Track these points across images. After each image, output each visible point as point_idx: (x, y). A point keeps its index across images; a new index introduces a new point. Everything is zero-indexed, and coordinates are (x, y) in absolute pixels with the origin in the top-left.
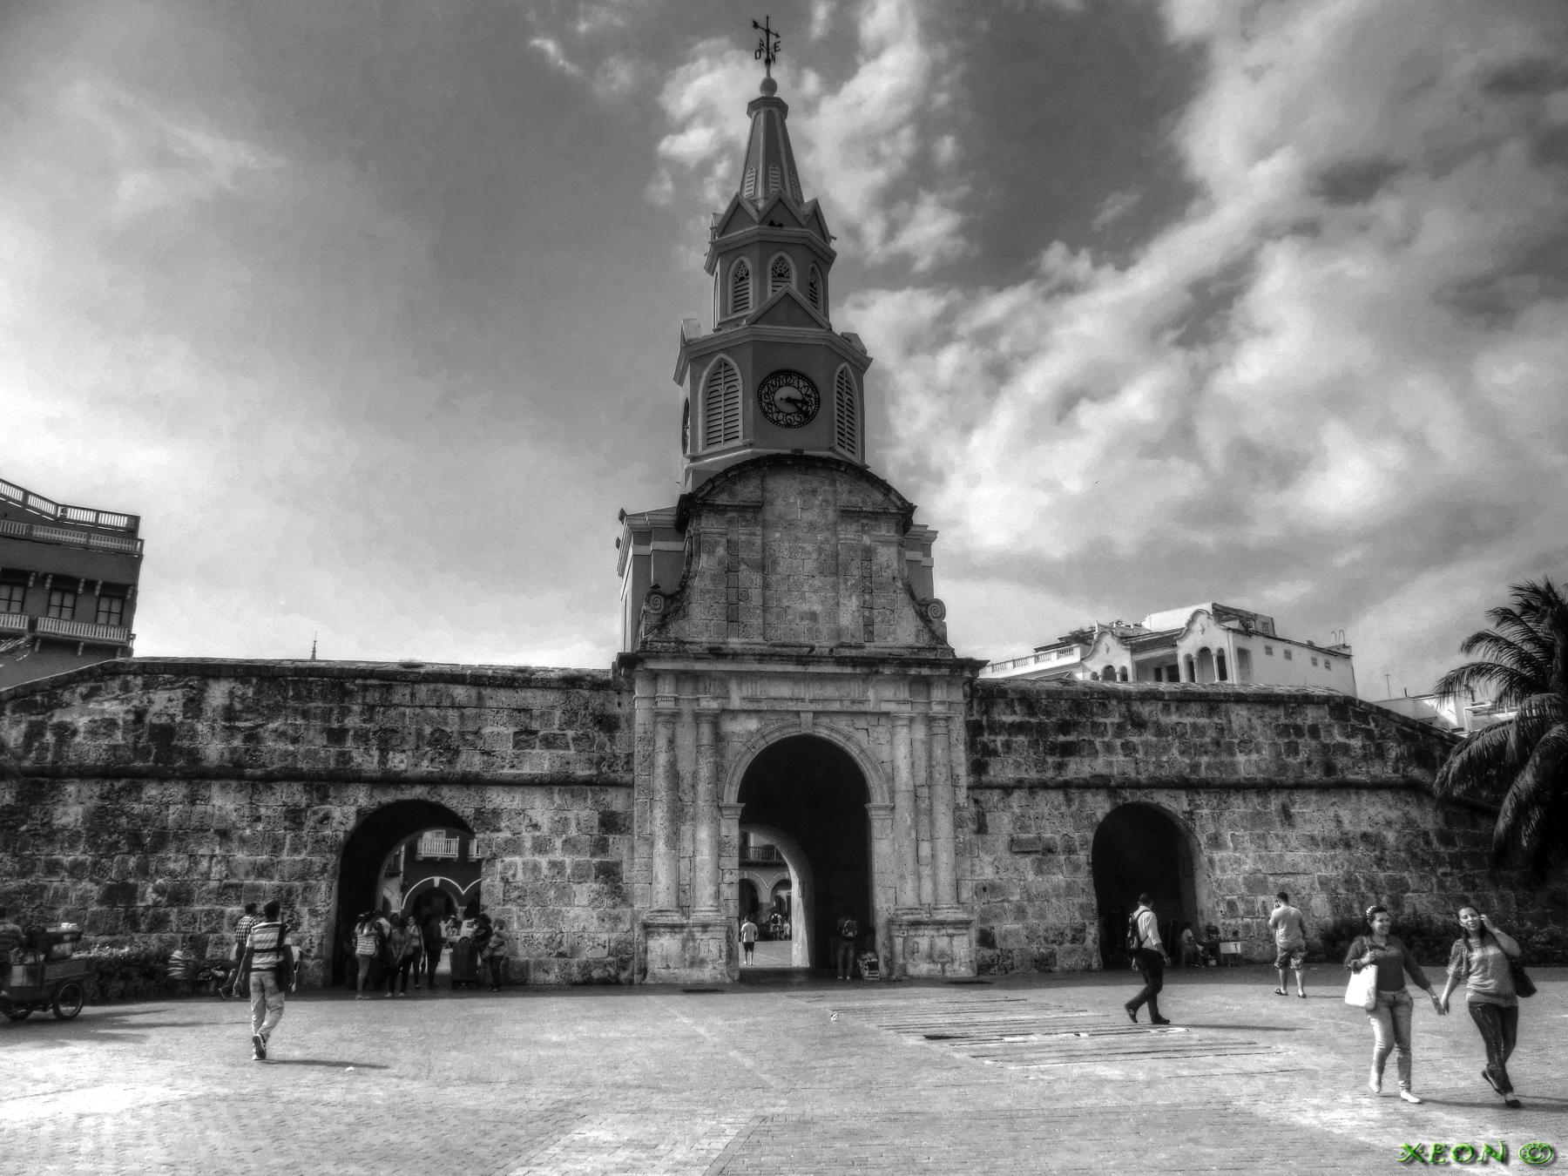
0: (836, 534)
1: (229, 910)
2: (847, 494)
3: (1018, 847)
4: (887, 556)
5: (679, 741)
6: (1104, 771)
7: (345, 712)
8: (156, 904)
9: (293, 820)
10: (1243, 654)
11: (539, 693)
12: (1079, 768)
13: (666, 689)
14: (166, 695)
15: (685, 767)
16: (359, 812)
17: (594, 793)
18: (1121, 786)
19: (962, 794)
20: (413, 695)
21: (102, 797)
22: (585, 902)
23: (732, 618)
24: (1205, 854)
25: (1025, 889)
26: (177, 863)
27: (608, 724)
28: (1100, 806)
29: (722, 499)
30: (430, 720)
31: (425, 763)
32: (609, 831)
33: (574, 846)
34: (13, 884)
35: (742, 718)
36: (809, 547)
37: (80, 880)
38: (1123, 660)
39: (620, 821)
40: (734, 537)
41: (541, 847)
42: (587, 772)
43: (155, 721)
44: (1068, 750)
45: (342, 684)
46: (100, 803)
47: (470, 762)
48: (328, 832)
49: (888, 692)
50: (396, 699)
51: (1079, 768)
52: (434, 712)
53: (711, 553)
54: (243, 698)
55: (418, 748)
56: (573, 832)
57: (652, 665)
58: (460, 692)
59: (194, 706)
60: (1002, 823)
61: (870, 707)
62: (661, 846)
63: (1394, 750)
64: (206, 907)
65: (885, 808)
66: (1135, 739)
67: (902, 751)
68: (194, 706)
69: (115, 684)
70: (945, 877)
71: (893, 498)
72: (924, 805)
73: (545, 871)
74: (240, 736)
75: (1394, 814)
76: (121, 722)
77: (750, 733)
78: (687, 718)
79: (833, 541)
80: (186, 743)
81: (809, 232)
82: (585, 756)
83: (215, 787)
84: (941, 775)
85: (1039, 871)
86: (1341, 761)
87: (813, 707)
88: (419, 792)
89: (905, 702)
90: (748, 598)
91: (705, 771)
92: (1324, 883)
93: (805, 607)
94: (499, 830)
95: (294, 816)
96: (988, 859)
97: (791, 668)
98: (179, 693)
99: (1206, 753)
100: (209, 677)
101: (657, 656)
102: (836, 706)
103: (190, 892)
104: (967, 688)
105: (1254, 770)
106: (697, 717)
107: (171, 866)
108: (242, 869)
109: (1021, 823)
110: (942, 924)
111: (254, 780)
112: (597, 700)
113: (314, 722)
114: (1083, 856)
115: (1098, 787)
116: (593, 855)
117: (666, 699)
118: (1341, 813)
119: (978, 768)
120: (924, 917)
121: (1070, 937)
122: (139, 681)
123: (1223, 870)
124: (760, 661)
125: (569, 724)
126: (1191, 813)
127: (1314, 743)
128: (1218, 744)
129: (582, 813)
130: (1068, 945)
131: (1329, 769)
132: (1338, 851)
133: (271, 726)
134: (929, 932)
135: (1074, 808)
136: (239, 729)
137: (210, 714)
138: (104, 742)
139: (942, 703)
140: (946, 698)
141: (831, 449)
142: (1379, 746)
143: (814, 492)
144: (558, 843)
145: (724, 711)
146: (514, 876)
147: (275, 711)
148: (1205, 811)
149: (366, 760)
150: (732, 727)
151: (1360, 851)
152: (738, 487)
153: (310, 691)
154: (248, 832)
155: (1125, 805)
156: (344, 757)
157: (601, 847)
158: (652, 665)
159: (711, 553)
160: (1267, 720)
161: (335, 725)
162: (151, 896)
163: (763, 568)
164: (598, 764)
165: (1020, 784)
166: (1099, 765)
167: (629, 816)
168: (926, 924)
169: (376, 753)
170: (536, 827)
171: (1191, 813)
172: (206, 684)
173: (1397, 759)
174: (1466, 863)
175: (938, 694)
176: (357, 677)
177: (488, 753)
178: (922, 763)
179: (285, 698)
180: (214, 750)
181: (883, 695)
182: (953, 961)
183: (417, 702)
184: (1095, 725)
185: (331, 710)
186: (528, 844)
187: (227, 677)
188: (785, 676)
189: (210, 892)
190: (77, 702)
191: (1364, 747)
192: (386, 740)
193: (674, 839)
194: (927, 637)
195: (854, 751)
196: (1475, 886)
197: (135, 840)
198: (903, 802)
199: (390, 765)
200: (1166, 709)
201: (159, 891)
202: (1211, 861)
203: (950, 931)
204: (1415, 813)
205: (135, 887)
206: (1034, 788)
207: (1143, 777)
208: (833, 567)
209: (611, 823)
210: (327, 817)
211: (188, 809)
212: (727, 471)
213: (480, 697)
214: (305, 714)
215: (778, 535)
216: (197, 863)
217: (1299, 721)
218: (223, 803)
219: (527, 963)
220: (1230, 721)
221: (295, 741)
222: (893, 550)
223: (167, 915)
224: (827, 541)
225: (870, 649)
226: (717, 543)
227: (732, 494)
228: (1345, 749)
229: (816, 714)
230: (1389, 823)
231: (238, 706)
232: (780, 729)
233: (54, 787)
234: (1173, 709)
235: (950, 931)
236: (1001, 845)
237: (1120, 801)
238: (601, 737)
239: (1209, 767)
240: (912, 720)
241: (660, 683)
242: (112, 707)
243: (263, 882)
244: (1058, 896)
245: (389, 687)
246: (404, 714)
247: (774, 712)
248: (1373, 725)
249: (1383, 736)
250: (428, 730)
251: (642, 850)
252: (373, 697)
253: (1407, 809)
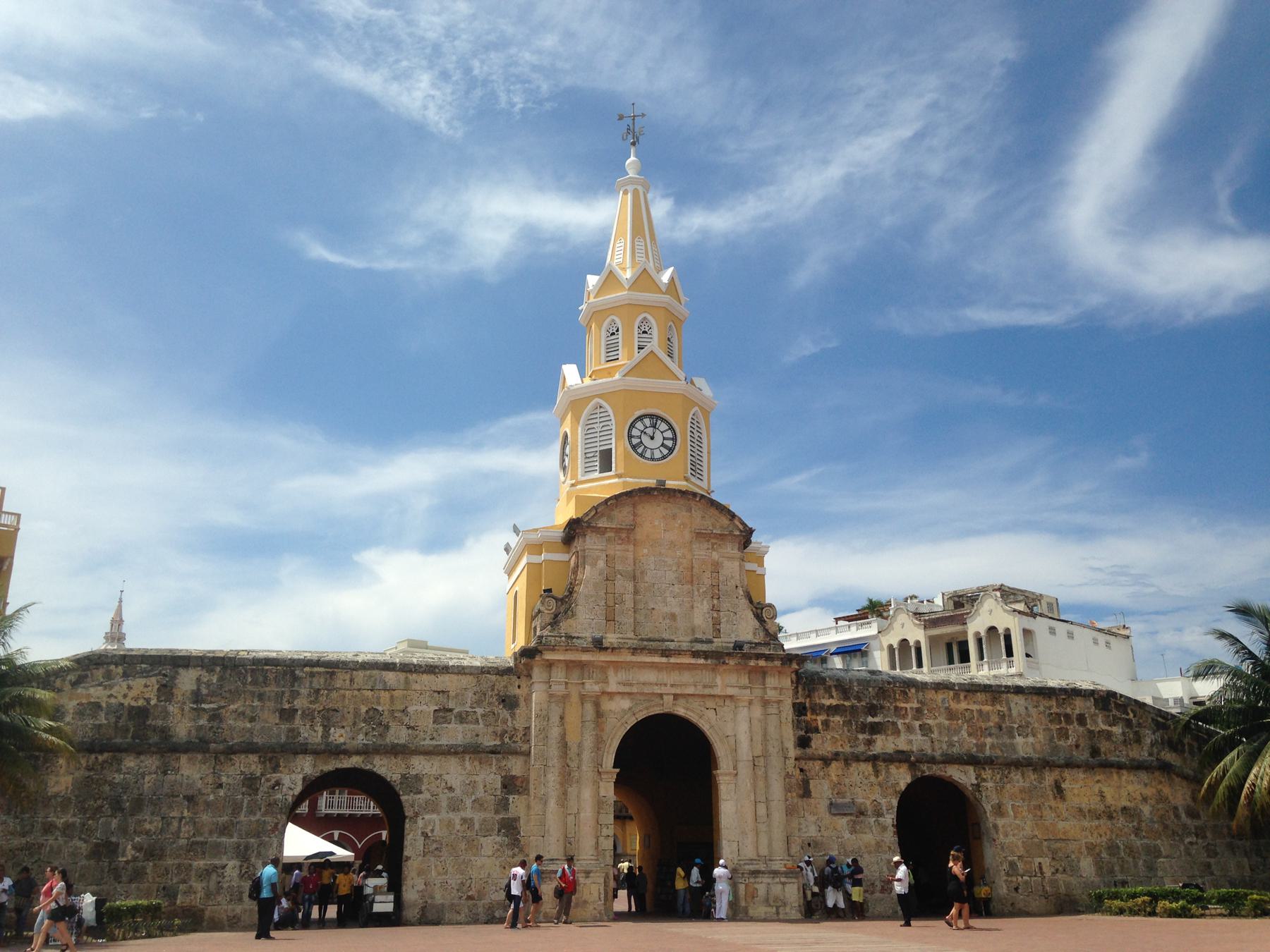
0: (691, 550)
1: (195, 864)
2: (699, 518)
3: (836, 809)
4: (731, 568)
5: (568, 719)
6: (903, 746)
7: (295, 695)
8: (135, 859)
9: (249, 787)
10: (1027, 633)
11: (455, 677)
12: (883, 744)
13: (559, 675)
14: (143, 681)
15: (572, 739)
16: (304, 779)
17: (498, 760)
18: (919, 761)
19: (791, 762)
20: (352, 680)
21: (89, 769)
22: (490, 853)
23: (610, 619)
24: (991, 818)
25: (842, 845)
26: (152, 824)
27: (510, 703)
28: (902, 777)
29: (602, 523)
30: (365, 701)
31: (361, 736)
32: (509, 793)
33: (481, 805)
34: (16, 842)
35: (618, 698)
36: (670, 561)
37: (72, 838)
38: (916, 634)
39: (518, 783)
40: (611, 552)
41: (455, 806)
42: (492, 743)
43: (133, 704)
44: (875, 729)
45: (293, 672)
46: (87, 774)
47: (398, 735)
48: (279, 796)
49: (732, 679)
50: (338, 684)
51: (883, 744)
52: (369, 693)
53: (594, 565)
54: (208, 685)
55: (354, 724)
56: (480, 793)
57: (549, 656)
58: (390, 677)
59: (166, 690)
60: (822, 789)
61: (717, 691)
62: (552, 804)
63: (1149, 737)
64: (176, 862)
65: (730, 774)
66: (929, 722)
67: (743, 728)
68: (166, 690)
69: (99, 673)
70: (778, 835)
71: (737, 523)
72: (760, 772)
73: (458, 827)
74: (206, 717)
75: (1149, 792)
76: (104, 705)
77: (624, 710)
78: (575, 698)
79: (689, 557)
80: (160, 723)
81: (667, 298)
82: (491, 729)
83: (184, 758)
84: (773, 750)
85: (853, 831)
86: (1104, 746)
87: (674, 691)
88: (355, 761)
89: (745, 688)
90: (622, 602)
91: (589, 742)
92: (1091, 848)
93: (666, 610)
94: (421, 792)
95: (251, 783)
96: (813, 819)
97: (657, 659)
98: (153, 680)
99: (990, 735)
100: (179, 666)
101: (553, 649)
102: (691, 690)
103: (162, 849)
104: (794, 676)
105: (1030, 750)
106: (583, 698)
107: (147, 826)
108: (206, 829)
109: (838, 789)
110: (775, 873)
111: (217, 754)
112: (501, 682)
113: (268, 704)
114: (889, 819)
115: (900, 761)
116: (497, 812)
117: (559, 683)
118: (1104, 789)
119: (803, 742)
120: (762, 867)
121: (879, 888)
122: (120, 670)
123: (1006, 835)
124: (633, 654)
125: (479, 703)
126: (978, 785)
127: (1081, 729)
128: (1000, 728)
129: (489, 777)
130: (878, 895)
131: (1095, 752)
132: (1102, 821)
133: (232, 707)
134: (766, 879)
135: (881, 778)
136: (204, 710)
137: (180, 698)
138: (90, 722)
139: (775, 688)
140: (780, 686)
141: (686, 479)
142: (1136, 733)
143: (674, 517)
144: (468, 803)
145: (603, 693)
146: (432, 831)
147: (235, 694)
148: (990, 784)
149: (312, 734)
150: (607, 705)
151: (1121, 821)
152: (615, 513)
153: (266, 678)
154: (212, 797)
155: (923, 777)
156: (293, 733)
157: (503, 805)
158: (549, 656)
159: (594, 565)
160: (1041, 709)
161: (287, 706)
162: (130, 852)
163: (634, 578)
164: (502, 736)
165: (836, 756)
166: (902, 743)
167: (526, 780)
168: (763, 873)
169: (320, 729)
170: (451, 789)
171: (978, 785)
172: (177, 673)
173: (1152, 745)
174: (1209, 834)
175: (771, 681)
176: (305, 665)
177: (413, 728)
178: (758, 738)
179: (244, 684)
180: (182, 728)
181: (727, 681)
182: (785, 905)
183: (355, 686)
184: (896, 708)
185: (283, 693)
186: (444, 804)
187: (195, 667)
188: (653, 666)
189: (181, 848)
190: (67, 687)
191: (1124, 733)
192: (329, 718)
193: (564, 797)
194: (762, 634)
195: (704, 726)
196: (1216, 854)
197: (117, 806)
198: (745, 770)
199: (331, 739)
200: (956, 697)
201: (138, 848)
202: (995, 826)
203: (783, 880)
204: (1166, 791)
205: (117, 845)
206: (850, 759)
207: (938, 754)
208: (689, 578)
209: (511, 785)
210: (278, 783)
211: (160, 777)
212: (607, 500)
213: (407, 682)
214: (261, 697)
215: (645, 551)
216: (168, 825)
217: (1069, 710)
218: (191, 771)
219: (443, 905)
220: (1010, 709)
221: (252, 720)
222: (737, 564)
223: (144, 868)
224: (684, 557)
225: (718, 644)
226: (598, 558)
227: (610, 518)
228: (1109, 735)
229: (676, 696)
230: (1145, 799)
231: (204, 691)
232: (647, 708)
233: (46, 761)
234: (962, 697)
235: (783, 880)
236: (823, 806)
237: (919, 774)
238: (505, 714)
239: (992, 746)
240: (750, 702)
241: (554, 670)
242: (96, 693)
243: (224, 839)
244: (870, 853)
245: (333, 674)
246: (344, 696)
247: (642, 694)
248: (1131, 715)
249: (1139, 725)
250: (364, 709)
251: (537, 808)
252: (318, 682)
253: (1160, 787)
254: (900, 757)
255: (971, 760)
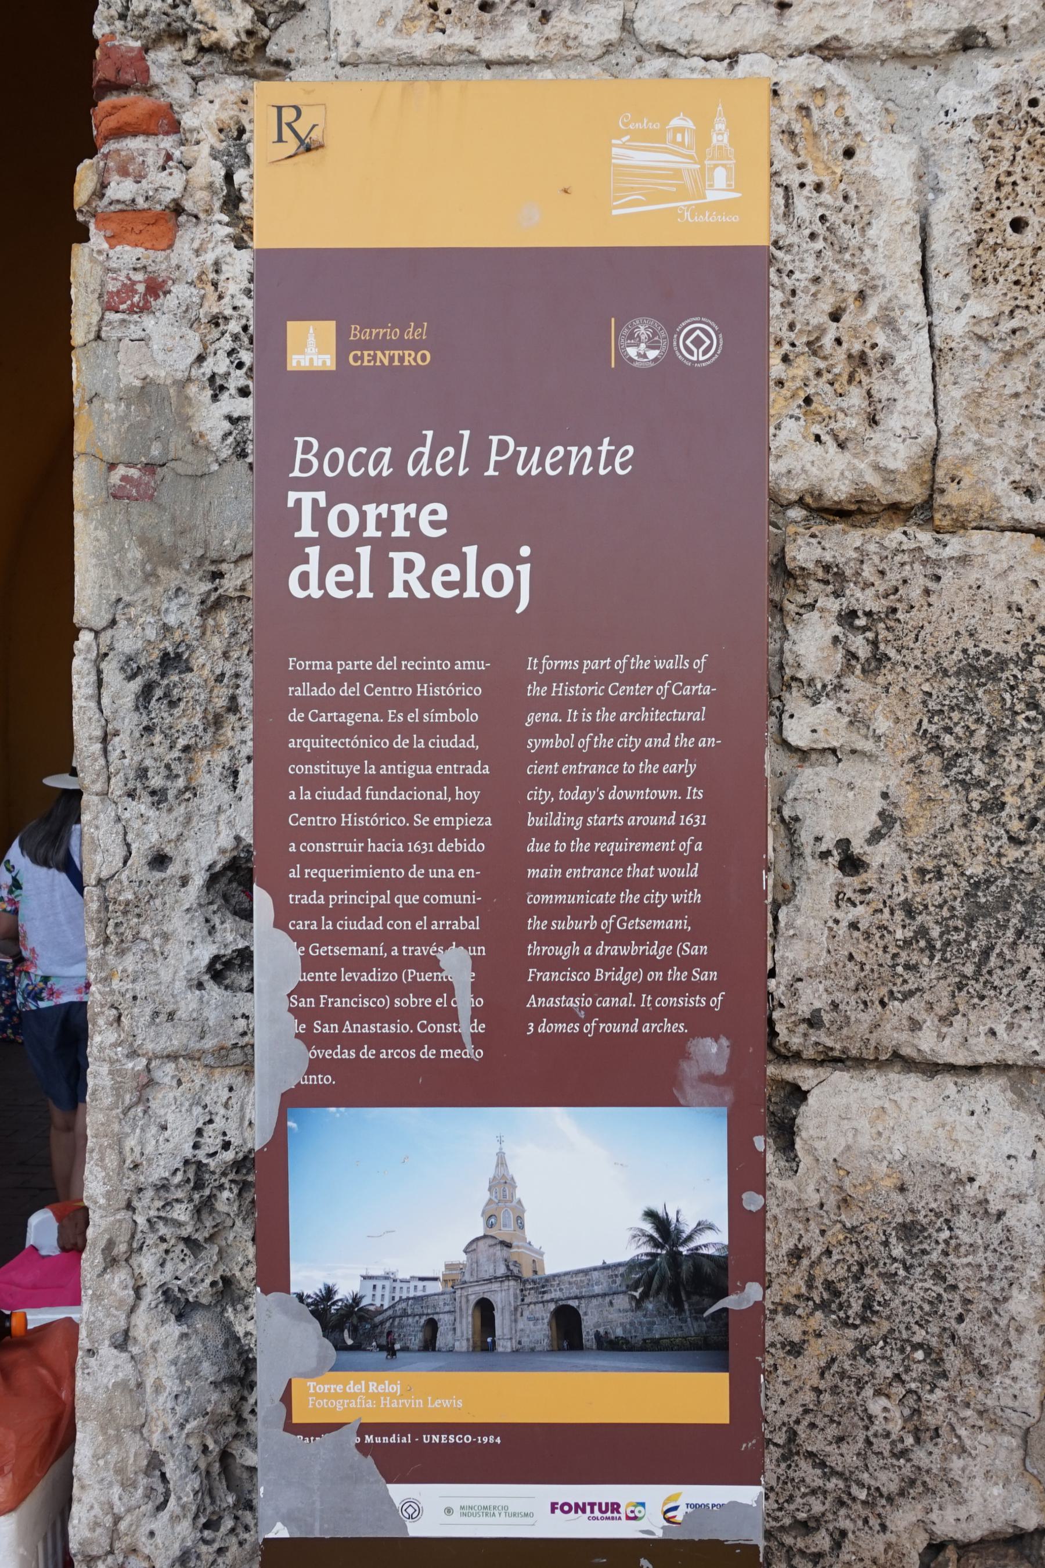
3: (529, 1319)
28: (552, 1307)
60: (526, 1314)
114: (546, 1321)
181: (495, 1286)
254: (552, 1300)
255: (576, 1298)
